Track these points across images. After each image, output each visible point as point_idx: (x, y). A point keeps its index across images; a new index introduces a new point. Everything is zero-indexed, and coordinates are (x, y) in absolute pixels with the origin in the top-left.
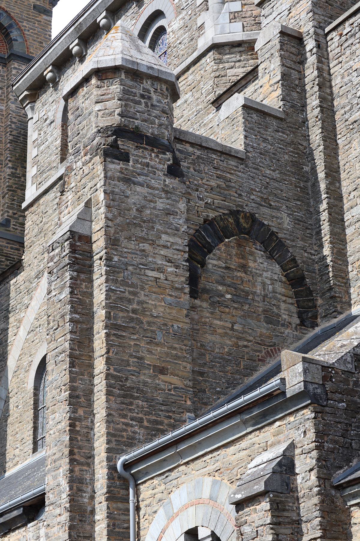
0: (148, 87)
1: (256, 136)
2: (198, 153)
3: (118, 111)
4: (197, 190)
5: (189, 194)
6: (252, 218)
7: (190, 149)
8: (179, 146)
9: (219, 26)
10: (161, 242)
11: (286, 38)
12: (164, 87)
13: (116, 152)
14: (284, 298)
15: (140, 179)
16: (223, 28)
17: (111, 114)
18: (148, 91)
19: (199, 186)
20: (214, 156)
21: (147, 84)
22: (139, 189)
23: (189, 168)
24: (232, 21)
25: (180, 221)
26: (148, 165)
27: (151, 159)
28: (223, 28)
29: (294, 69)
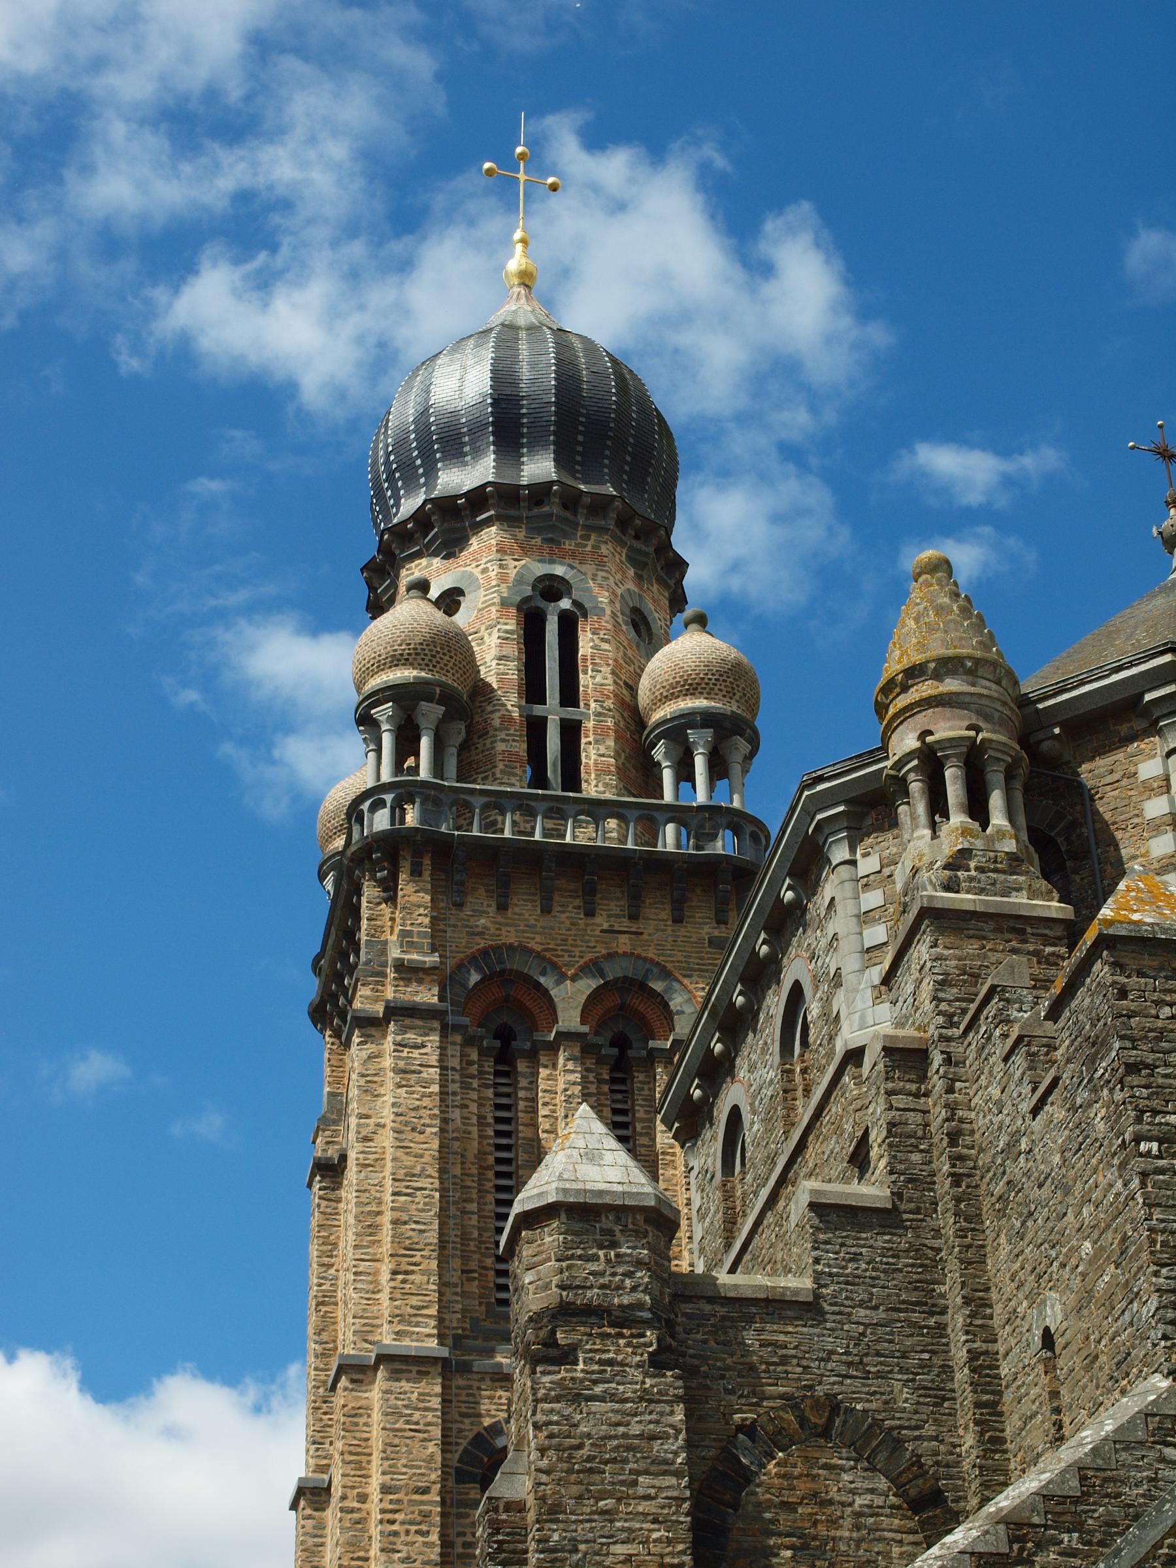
0: (610, 1225)
1: (836, 1253)
2: (722, 1311)
3: (555, 1280)
4: (723, 1377)
5: (708, 1388)
6: (833, 1406)
7: (708, 1308)
8: (688, 1308)
9: (857, 1015)
10: (641, 1491)
11: (897, 1057)
12: (640, 1218)
13: (553, 1352)
14: (898, 1536)
15: (598, 1389)
16: (863, 1018)
17: (547, 1287)
18: (611, 1232)
19: (727, 1368)
20: (754, 1310)
21: (608, 1222)
22: (596, 1406)
23: (705, 1342)
24: (879, 1001)
25: (674, 1449)
26: (610, 1363)
27: (617, 1352)
28: (863, 1018)
29: (914, 1110)
